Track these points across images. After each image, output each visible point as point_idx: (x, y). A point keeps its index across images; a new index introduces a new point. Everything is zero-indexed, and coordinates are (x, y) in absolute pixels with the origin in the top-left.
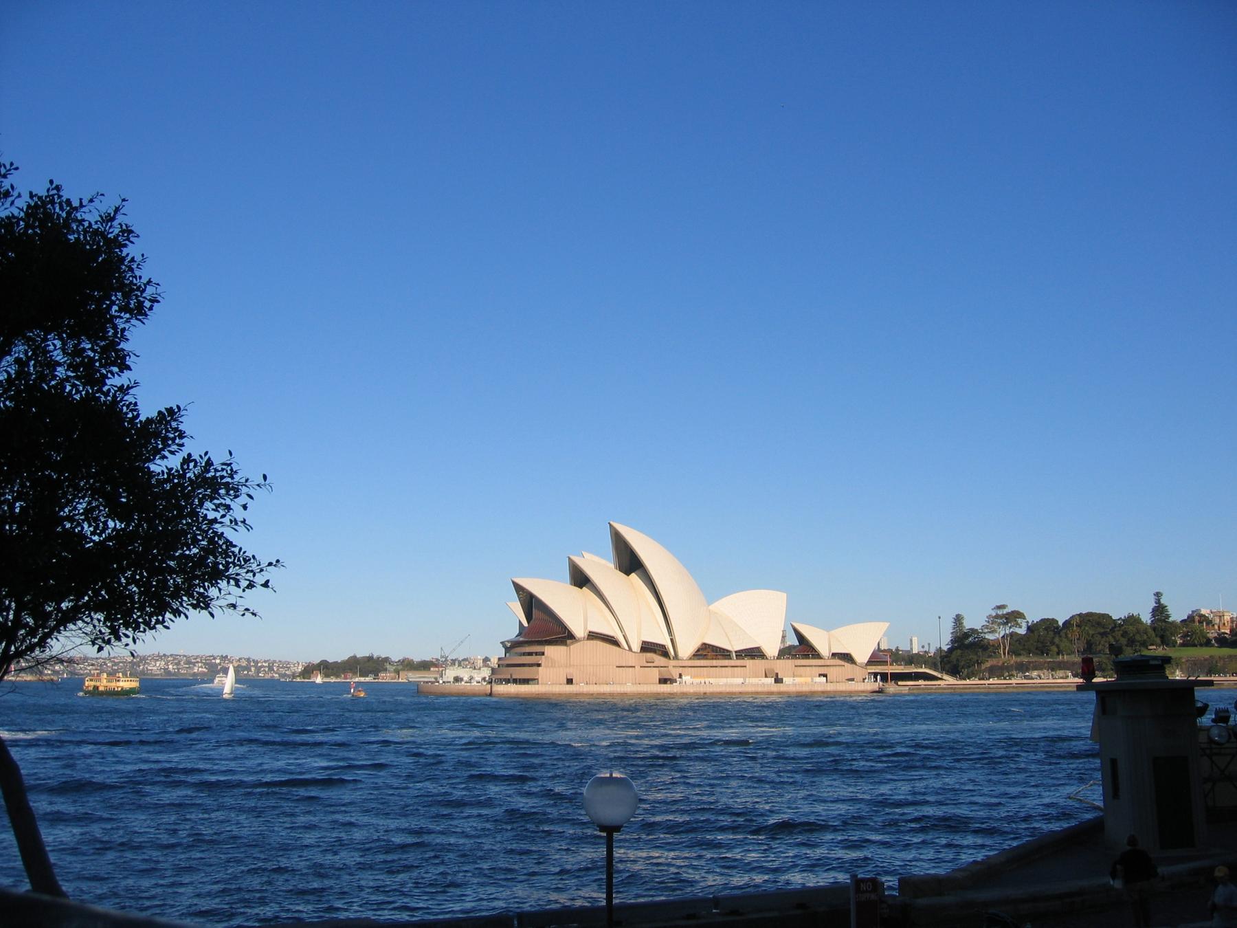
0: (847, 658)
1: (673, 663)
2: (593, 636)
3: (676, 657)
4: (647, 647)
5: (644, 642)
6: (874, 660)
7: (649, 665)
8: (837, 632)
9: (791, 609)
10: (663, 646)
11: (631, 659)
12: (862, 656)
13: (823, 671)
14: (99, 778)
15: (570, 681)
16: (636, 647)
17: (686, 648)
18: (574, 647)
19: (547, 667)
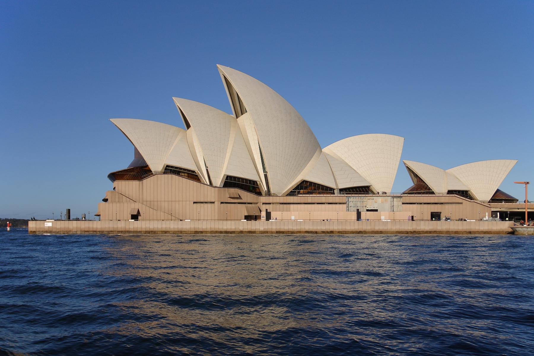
0: (465, 194)
1: (263, 199)
2: (170, 170)
3: (269, 193)
4: (231, 182)
5: (228, 177)
6: (499, 197)
7: (237, 200)
8: (454, 171)
9: (406, 153)
10: (255, 182)
11: (211, 194)
12: (483, 193)
13: (436, 209)
14: (46, 282)
15: (135, 217)
16: (218, 181)
17: (281, 183)
18: (148, 182)
19: (112, 202)
